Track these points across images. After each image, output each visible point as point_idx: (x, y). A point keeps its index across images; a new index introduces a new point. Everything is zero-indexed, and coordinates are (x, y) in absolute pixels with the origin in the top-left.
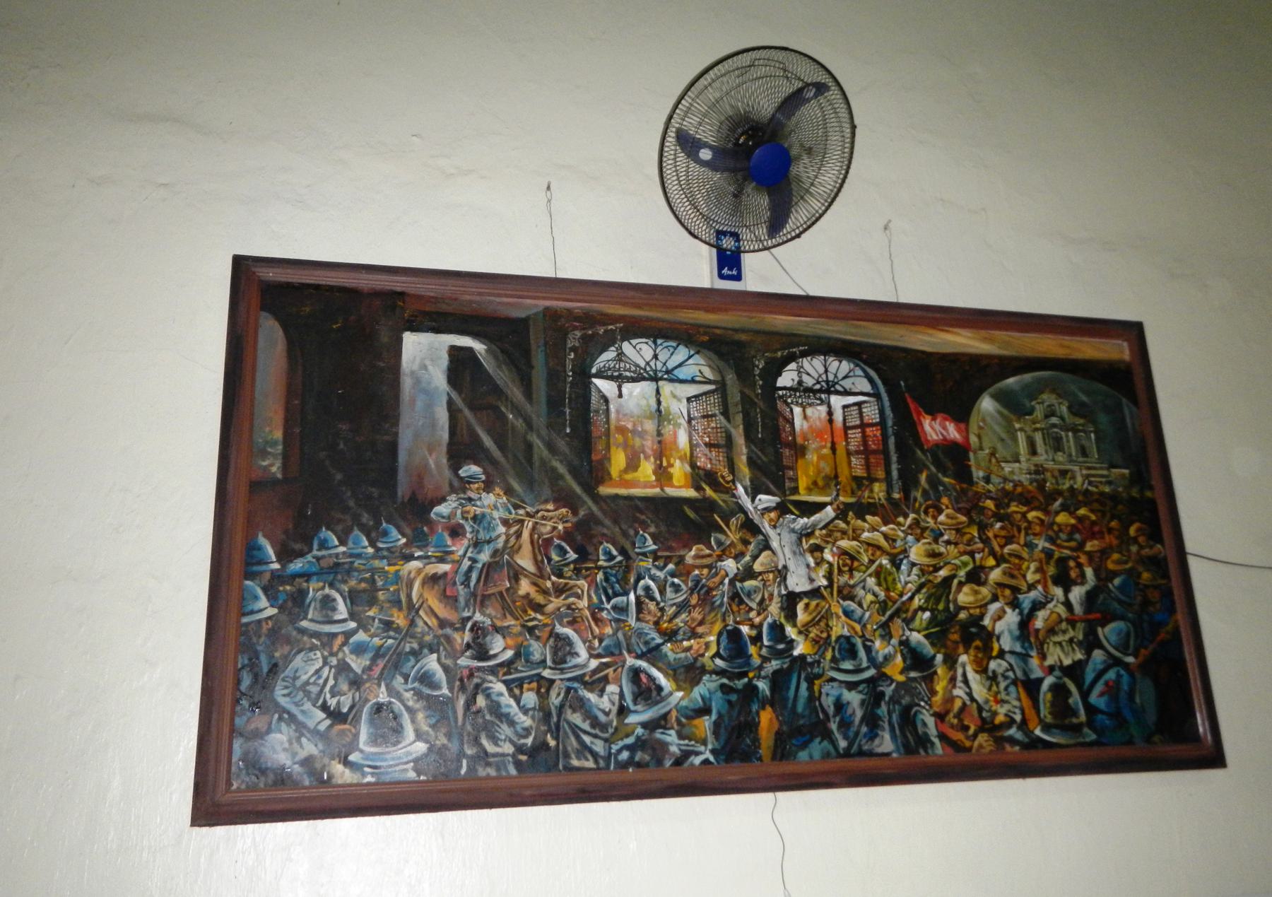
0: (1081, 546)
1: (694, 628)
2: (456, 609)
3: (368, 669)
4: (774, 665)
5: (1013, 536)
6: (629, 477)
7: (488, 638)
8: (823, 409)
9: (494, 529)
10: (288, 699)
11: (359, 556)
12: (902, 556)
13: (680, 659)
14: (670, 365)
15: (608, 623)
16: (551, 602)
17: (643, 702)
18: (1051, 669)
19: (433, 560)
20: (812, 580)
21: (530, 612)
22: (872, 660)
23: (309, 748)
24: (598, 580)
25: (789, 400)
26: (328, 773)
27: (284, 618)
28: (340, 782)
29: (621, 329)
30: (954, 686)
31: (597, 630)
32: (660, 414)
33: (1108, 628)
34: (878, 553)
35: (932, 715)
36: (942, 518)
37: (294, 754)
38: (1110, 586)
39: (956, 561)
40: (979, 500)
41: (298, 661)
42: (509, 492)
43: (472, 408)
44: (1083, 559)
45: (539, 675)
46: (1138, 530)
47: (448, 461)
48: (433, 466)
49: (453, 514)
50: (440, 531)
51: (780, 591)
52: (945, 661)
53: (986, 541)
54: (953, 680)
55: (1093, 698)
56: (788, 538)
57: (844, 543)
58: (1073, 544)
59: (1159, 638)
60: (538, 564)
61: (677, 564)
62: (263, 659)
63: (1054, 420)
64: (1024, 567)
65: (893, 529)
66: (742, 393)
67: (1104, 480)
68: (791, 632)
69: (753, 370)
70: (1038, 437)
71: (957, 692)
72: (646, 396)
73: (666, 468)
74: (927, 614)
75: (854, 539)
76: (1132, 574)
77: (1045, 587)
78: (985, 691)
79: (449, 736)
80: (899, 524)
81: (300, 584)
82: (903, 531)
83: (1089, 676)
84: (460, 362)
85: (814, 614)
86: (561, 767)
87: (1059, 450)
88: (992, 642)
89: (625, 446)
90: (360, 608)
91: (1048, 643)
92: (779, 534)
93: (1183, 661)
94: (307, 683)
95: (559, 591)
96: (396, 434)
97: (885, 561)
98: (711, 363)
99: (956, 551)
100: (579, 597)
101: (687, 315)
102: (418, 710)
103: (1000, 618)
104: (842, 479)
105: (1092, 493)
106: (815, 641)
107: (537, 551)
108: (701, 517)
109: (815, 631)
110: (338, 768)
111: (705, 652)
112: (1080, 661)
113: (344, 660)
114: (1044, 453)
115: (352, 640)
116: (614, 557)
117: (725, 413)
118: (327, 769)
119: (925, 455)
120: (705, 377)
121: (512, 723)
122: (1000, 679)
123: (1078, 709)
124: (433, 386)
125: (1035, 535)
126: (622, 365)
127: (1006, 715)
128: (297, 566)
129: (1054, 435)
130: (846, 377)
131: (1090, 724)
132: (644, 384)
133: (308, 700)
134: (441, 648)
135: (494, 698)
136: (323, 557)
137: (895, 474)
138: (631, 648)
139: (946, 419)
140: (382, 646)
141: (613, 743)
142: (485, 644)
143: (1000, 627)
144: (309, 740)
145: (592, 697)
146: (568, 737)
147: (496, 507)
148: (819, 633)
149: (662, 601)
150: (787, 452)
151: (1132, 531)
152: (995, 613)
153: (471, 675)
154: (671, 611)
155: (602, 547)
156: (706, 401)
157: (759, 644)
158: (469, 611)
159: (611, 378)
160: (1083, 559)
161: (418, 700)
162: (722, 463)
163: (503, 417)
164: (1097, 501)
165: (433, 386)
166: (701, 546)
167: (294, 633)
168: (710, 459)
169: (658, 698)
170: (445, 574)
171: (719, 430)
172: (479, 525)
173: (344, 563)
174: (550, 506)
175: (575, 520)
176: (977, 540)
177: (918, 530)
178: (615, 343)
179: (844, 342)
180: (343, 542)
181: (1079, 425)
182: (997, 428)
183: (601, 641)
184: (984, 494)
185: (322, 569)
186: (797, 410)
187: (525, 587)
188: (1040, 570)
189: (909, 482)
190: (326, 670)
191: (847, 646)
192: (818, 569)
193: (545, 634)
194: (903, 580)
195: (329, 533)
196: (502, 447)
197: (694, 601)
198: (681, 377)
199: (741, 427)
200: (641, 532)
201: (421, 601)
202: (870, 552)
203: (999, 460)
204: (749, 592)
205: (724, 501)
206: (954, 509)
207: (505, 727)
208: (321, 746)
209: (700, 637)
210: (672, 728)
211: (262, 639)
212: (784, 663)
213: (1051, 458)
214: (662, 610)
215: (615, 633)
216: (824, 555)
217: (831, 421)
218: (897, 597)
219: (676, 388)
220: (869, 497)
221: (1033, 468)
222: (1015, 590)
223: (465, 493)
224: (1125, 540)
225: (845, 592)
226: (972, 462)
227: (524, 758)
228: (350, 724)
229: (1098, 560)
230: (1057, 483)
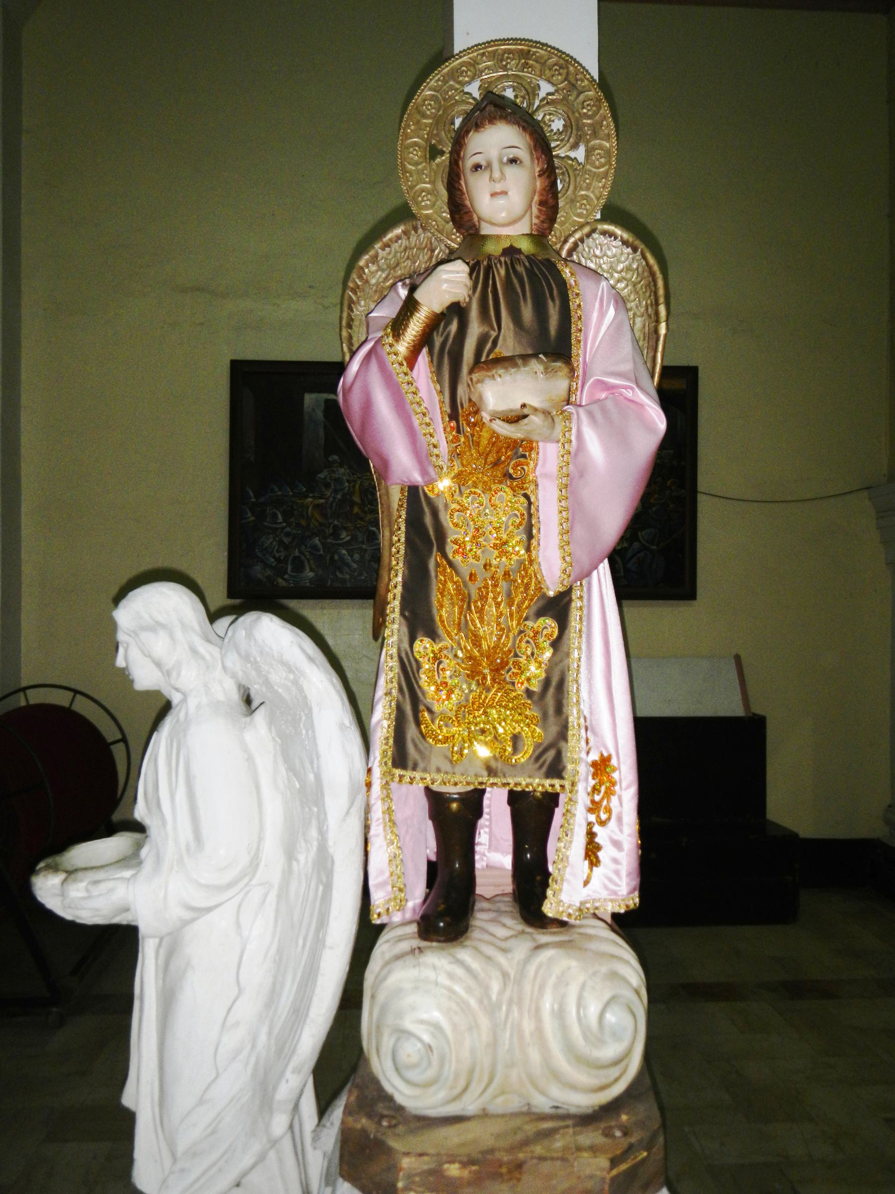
23: (269, 572)
42: (350, 467)
55: (630, 565)
60: (362, 500)
83: (630, 554)
110: (280, 580)
112: (626, 547)
115: (284, 531)
128: (262, 500)
151: (669, 483)
170: (322, 504)
187: (356, 510)
190: (274, 543)
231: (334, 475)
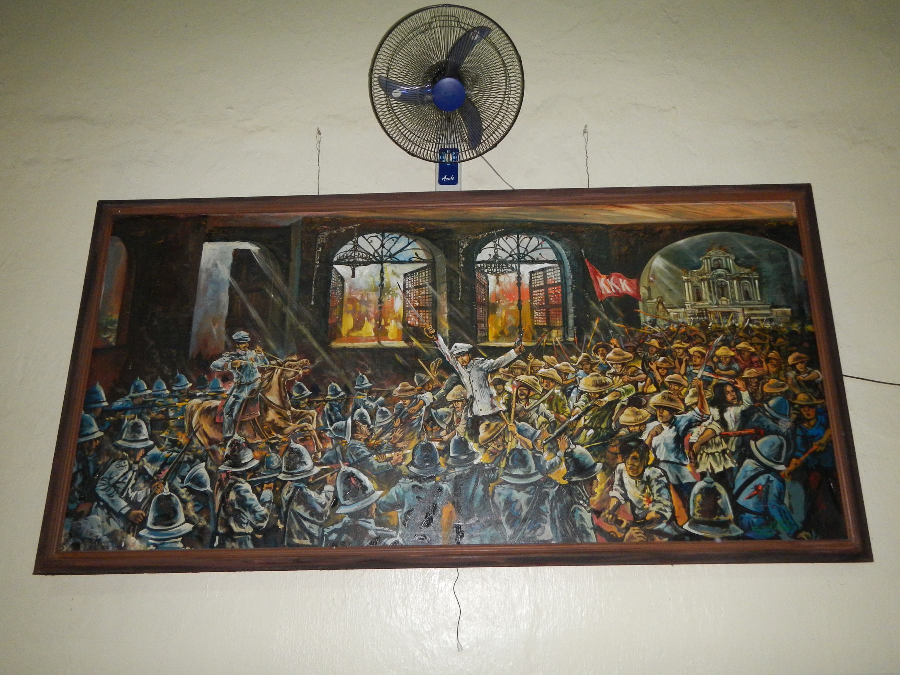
0: (739, 374)
1: (396, 444)
2: (222, 432)
3: (158, 473)
4: (458, 471)
5: (675, 368)
6: (354, 335)
7: (243, 451)
8: (513, 276)
9: (253, 375)
10: (104, 493)
11: (160, 396)
12: (572, 387)
13: (382, 467)
14: (393, 251)
15: (330, 441)
16: (290, 426)
17: (351, 499)
18: (703, 475)
19: (209, 398)
20: (493, 407)
21: (274, 433)
22: (540, 468)
24: (325, 409)
25: (486, 271)
26: (125, 543)
27: (106, 438)
28: (132, 549)
29: (358, 228)
30: (612, 489)
31: (321, 446)
32: (383, 289)
33: (759, 443)
34: (552, 384)
35: (589, 512)
36: (610, 355)
37: (104, 531)
38: (766, 406)
39: (621, 388)
40: (645, 339)
41: (113, 468)
42: (266, 349)
43: (247, 291)
44: (741, 385)
45: (276, 477)
46: (797, 359)
47: (226, 328)
48: (215, 333)
49: (226, 366)
50: (216, 378)
51: (466, 416)
52: (604, 469)
53: (648, 372)
54: (610, 485)
55: (742, 500)
56: (476, 375)
57: (523, 378)
58: (732, 372)
59: (811, 451)
61: (386, 397)
62: (91, 465)
63: (720, 271)
64: (683, 393)
65: (567, 366)
66: (448, 268)
67: (765, 318)
68: (473, 446)
69: (459, 249)
70: (704, 288)
71: (612, 494)
72: (373, 275)
73: (383, 327)
74: (592, 432)
75: (531, 375)
76: (789, 397)
77: (702, 408)
78: (640, 493)
79: (208, 521)
80: (573, 361)
81: (120, 416)
82: (574, 367)
83: (739, 482)
84: (241, 260)
85: (494, 433)
86: (286, 544)
87: (723, 296)
88: (649, 453)
89: (354, 312)
90: (157, 432)
91: (702, 455)
92: (470, 373)
93: (834, 469)
94: (118, 482)
95: (296, 418)
96: (193, 313)
97: (557, 391)
98: (425, 247)
99: (621, 380)
100: (310, 422)
101: (410, 214)
102: (190, 502)
103: (657, 434)
104: (526, 328)
105: (753, 330)
106: (493, 454)
107: (282, 390)
108: (409, 362)
109: (493, 446)
111: (403, 462)
112: (731, 469)
113: (143, 467)
114: (708, 299)
115: (149, 454)
116: (339, 393)
117: (434, 284)
118: (125, 540)
119: (600, 307)
120: (420, 258)
121: (254, 512)
122: (654, 483)
123: (727, 508)
124: (221, 278)
125: (695, 366)
126: (357, 254)
127: (657, 513)
128: (119, 404)
129: (720, 284)
130: (532, 251)
131: (737, 521)
132: (372, 266)
133: (117, 493)
134: (209, 459)
135: (243, 494)
136: (137, 397)
137: (571, 322)
138: (345, 458)
139: (620, 277)
140: (169, 457)
141: (326, 528)
142: (240, 456)
143: (656, 441)
144: (115, 520)
145: (313, 494)
146: (293, 522)
147: (256, 360)
148: (496, 447)
149: (372, 424)
150: (481, 310)
151: (791, 360)
152: (653, 430)
153: (228, 478)
154: (378, 431)
155: (330, 386)
156: (419, 275)
157: (446, 456)
158: (230, 433)
159: (348, 264)
160: (741, 385)
161: (190, 495)
162: (427, 321)
163: (266, 297)
164: (757, 336)
165: (221, 278)
166: (406, 383)
167: (113, 448)
168: (419, 319)
169: (363, 496)
170: (217, 407)
171: (427, 297)
172: (243, 373)
173: (149, 402)
174: (295, 358)
175: (312, 367)
176: (641, 372)
177: (588, 366)
178: (354, 239)
179: (534, 223)
180: (150, 388)
181: (745, 274)
182: (667, 282)
183: (323, 454)
184: (651, 335)
185: (135, 405)
186: (492, 278)
187: (272, 415)
188: (698, 394)
189: (582, 326)
190: (131, 473)
191: (520, 458)
192: (499, 398)
193: (282, 450)
194: (572, 406)
195: (142, 381)
196: (264, 317)
197: (397, 425)
198: (401, 259)
199: (446, 293)
200: (361, 374)
201: (198, 426)
202: (545, 384)
203: (666, 307)
204: (442, 416)
205: (427, 349)
206: (622, 348)
207: (248, 514)
208: (122, 525)
209: (400, 451)
210: (372, 518)
211: (92, 453)
212: (466, 470)
213: (715, 302)
214: (372, 431)
215: (335, 447)
216: (506, 387)
217: (519, 284)
218: (566, 419)
219: (396, 268)
220: (547, 342)
221: (697, 312)
222: (674, 411)
223: (235, 351)
224: (782, 367)
225: (521, 416)
226: (641, 310)
227: (260, 537)
228: (143, 510)
229: (755, 386)
230: (720, 324)
231: (239, 362)
